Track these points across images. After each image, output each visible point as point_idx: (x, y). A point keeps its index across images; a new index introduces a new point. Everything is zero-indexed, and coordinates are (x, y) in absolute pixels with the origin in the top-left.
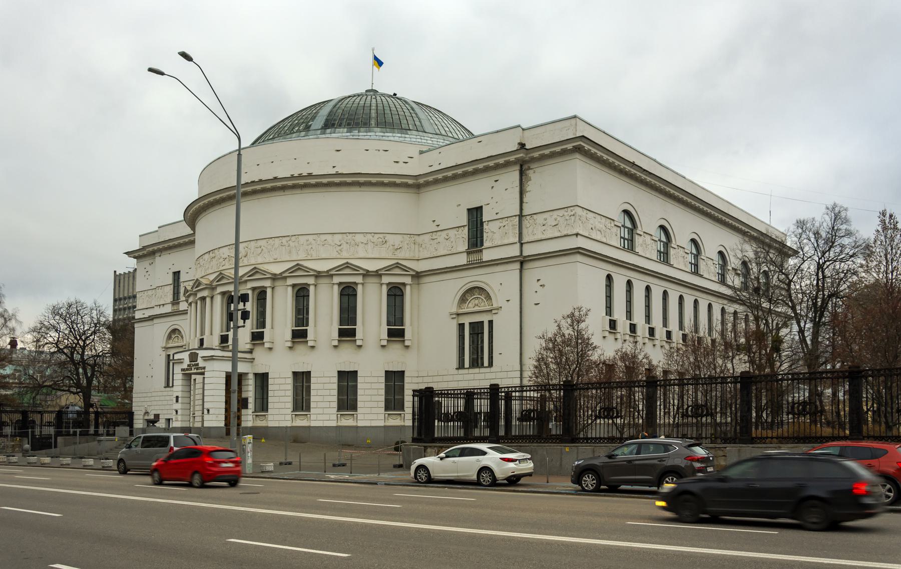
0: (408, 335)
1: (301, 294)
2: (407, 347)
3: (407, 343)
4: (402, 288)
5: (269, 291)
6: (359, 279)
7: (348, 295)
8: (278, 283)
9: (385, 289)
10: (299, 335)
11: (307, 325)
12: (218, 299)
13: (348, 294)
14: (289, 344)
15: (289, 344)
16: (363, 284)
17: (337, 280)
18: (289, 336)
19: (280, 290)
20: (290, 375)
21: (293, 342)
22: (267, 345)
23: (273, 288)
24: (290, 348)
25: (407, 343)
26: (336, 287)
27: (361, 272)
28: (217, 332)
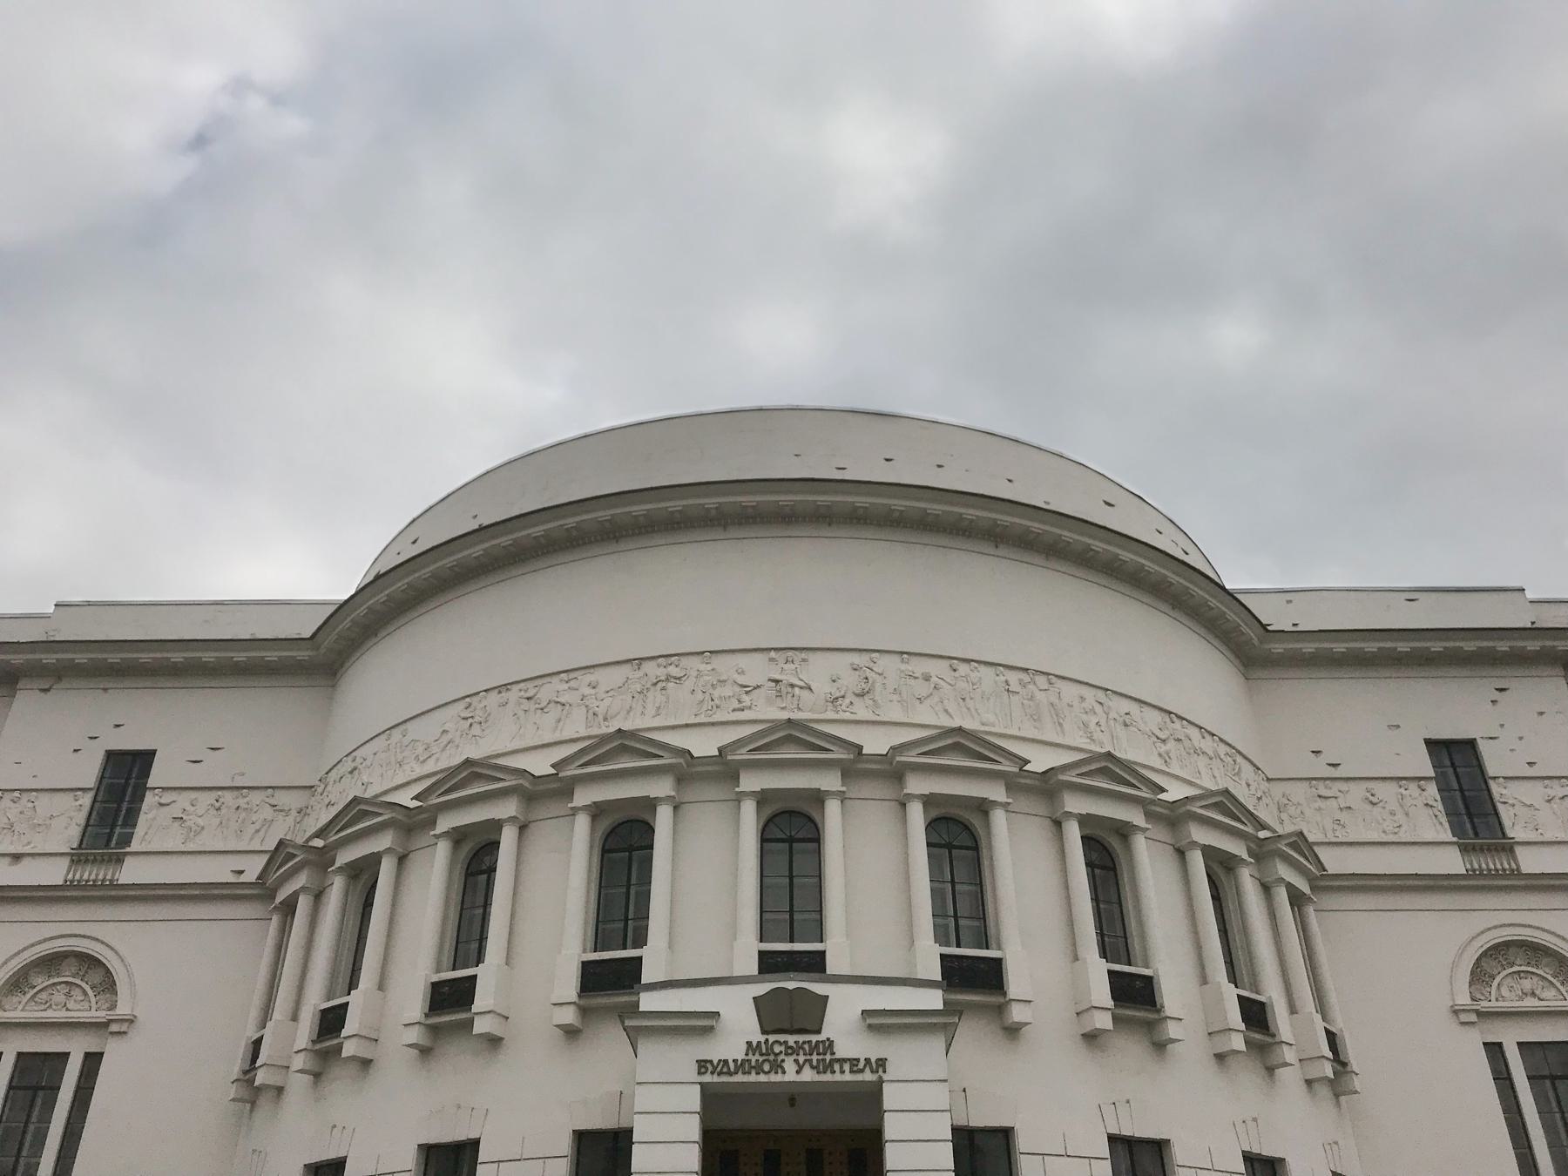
0: (1016, 984)
1: (625, 847)
2: (1013, 1031)
3: (1017, 1014)
4: (976, 821)
5: (508, 837)
6: (829, 781)
7: (791, 840)
8: (542, 811)
9: (917, 816)
10: (609, 980)
11: (641, 941)
12: (338, 885)
13: (791, 833)
14: (569, 1016)
15: (569, 1016)
16: (842, 797)
17: (751, 782)
18: (568, 986)
19: (546, 835)
20: (565, 1145)
21: (584, 1011)
22: (481, 1026)
23: (523, 828)
24: (571, 1032)
25: (1017, 1014)
26: (749, 809)
27: (838, 754)
28: (315, 1001)
